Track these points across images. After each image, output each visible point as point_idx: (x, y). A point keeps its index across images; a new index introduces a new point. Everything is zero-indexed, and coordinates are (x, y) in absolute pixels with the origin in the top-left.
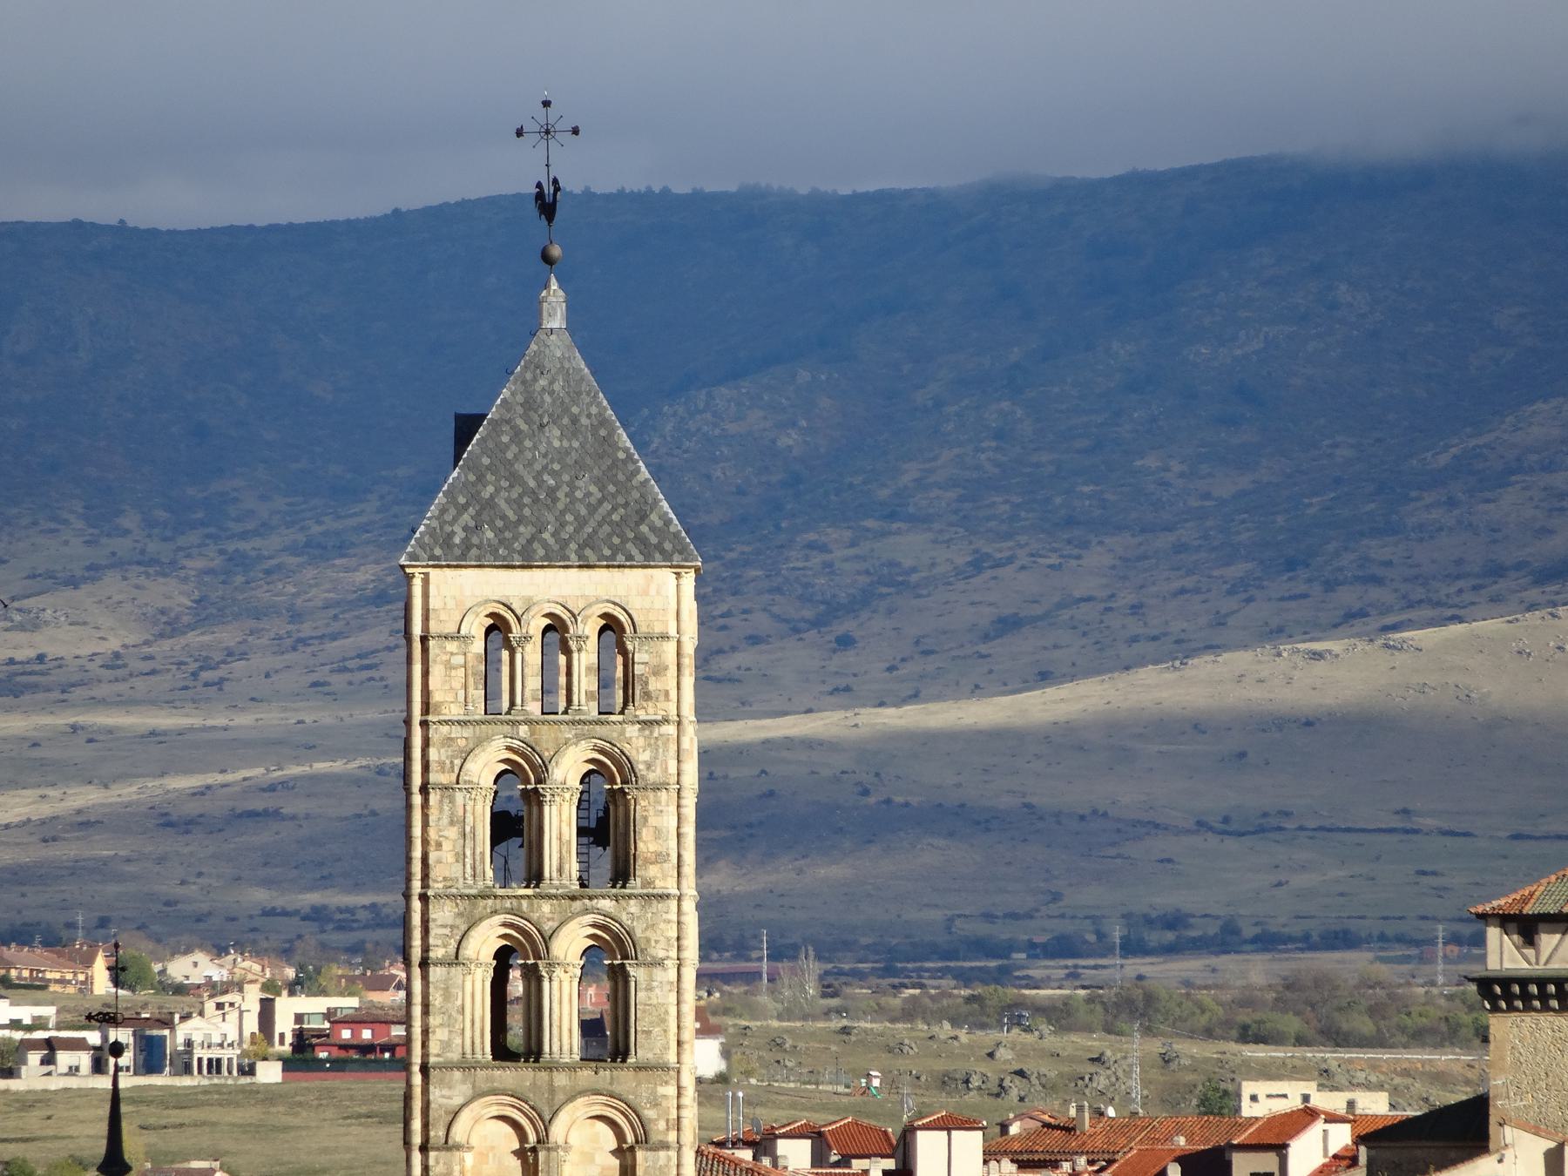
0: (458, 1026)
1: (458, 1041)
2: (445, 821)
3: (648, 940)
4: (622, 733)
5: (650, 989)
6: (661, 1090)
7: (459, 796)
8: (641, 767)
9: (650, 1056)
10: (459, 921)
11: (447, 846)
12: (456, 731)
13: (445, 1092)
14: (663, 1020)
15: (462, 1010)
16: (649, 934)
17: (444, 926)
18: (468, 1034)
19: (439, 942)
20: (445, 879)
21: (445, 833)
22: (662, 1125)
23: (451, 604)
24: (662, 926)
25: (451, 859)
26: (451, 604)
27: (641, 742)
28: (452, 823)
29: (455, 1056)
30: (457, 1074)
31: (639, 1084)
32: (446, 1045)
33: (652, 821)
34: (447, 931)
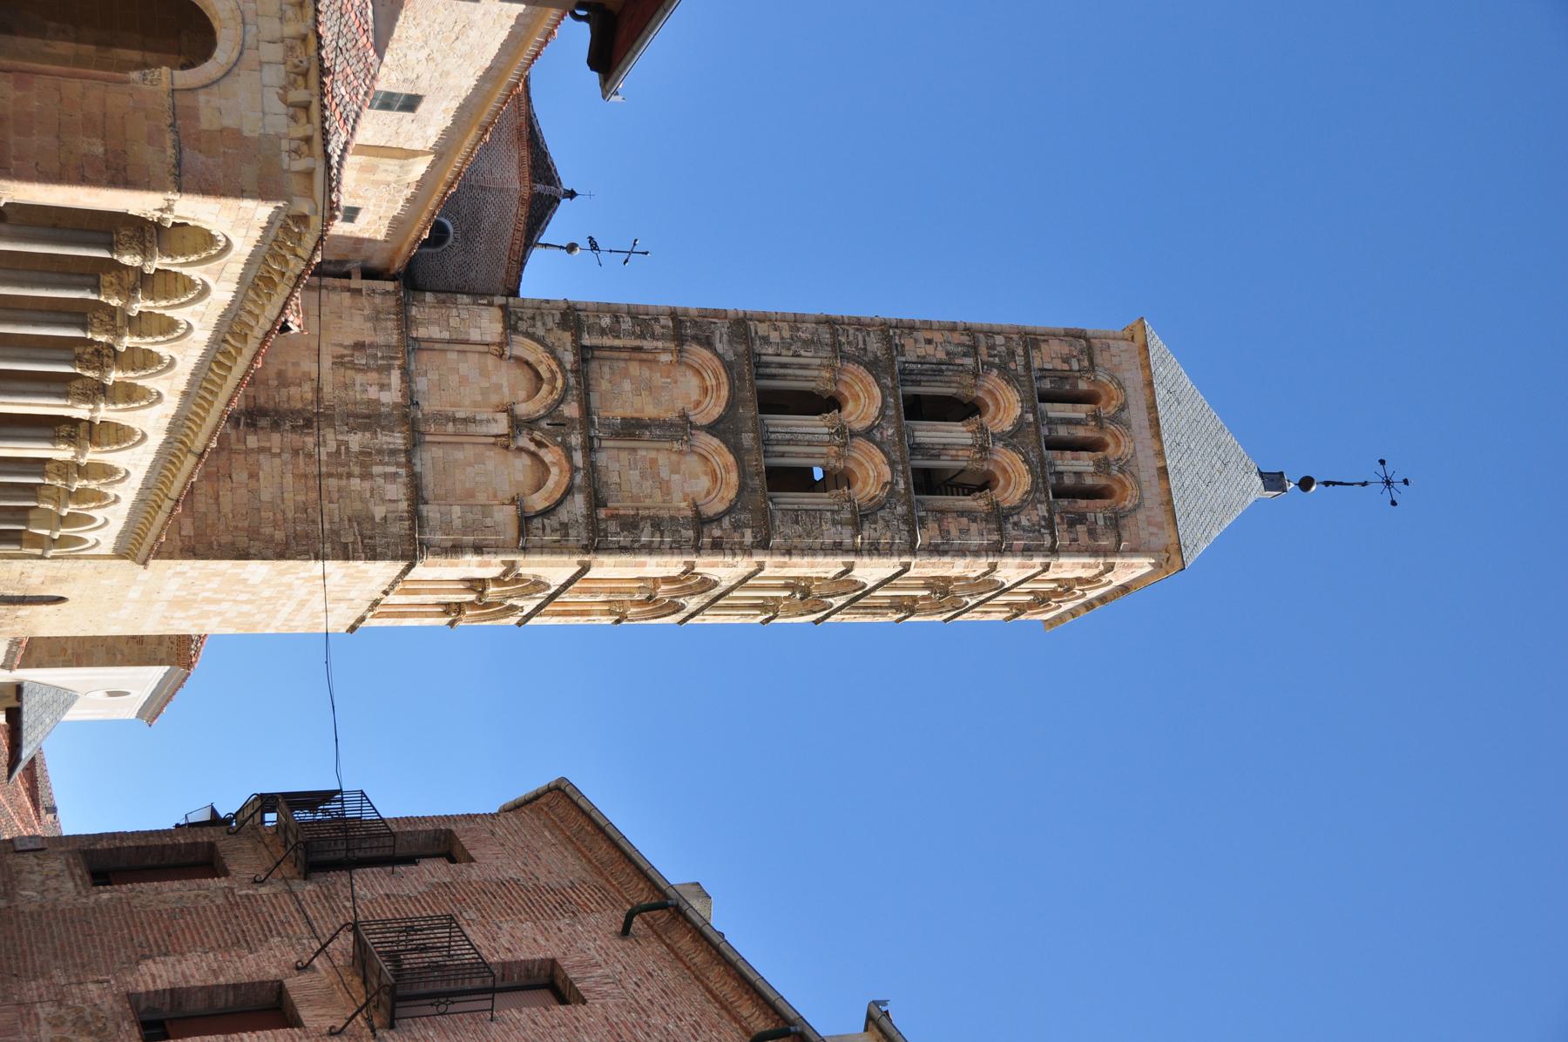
0: (784, 352)
1: (770, 351)
2: (951, 348)
3: (875, 522)
4: (1041, 502)
5: (835, 523)
6: (748, 533)
7: (969, 361)
8: (1016, 518)
10: (870, 355)
11: (930, 349)
12: (1020, 360)
13: (725, 337)
14: (808, 535)
15: (796, 355)
18: (777, 359)
22: (717, 533)
23: (1116, 360)
24: (889, 534)
25: (921, 352)
26: (1116, 360)
27: (1035, 519)
28: (948, 354)
29: (758, 347)
32: (766, 340)
33: (974, 527)
34: (861, 345)
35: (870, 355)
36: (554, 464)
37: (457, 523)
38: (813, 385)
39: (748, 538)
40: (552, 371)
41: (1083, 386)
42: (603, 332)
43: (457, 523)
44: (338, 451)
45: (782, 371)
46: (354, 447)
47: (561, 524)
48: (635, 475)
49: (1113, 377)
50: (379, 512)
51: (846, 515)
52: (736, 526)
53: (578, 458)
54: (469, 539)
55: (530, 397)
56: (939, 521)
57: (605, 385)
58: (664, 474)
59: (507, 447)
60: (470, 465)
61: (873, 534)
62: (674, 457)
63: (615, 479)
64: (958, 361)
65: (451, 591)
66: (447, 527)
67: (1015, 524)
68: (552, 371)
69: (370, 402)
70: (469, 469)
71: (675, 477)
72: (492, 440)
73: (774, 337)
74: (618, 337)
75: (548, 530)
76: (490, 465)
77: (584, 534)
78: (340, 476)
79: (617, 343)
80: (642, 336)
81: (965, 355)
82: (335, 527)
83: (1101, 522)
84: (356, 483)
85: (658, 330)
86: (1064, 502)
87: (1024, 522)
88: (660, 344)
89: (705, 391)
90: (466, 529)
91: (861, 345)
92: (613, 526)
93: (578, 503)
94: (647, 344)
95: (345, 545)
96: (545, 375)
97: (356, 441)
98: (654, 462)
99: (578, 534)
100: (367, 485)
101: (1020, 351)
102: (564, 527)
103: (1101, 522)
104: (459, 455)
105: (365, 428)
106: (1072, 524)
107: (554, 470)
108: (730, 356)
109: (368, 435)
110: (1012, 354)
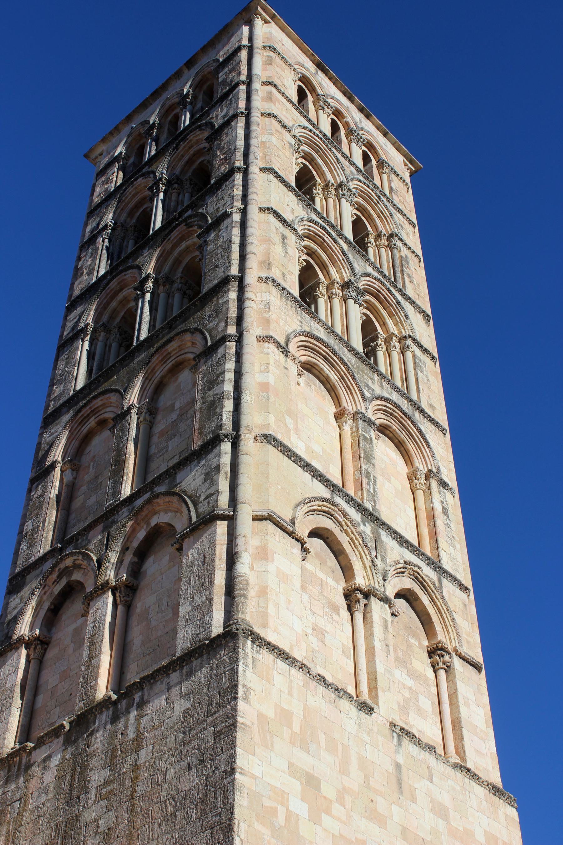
36: (148, 523)
38: (114, 345)
40: (60, 577)
44: (107, 797)
46: (106, 773)
50: (181, 706)
58: (174, 416)
65: (369, 635)
68: (60, 577)
69: (59, 778)
70: (153, 623)
71: (178, 405)
78: (135, 781)
82: (194, 761)
84: (144, 755)
95: (218, 735)
96: (64, 582)
97: (97, 776)
100: (148, 737)
105: (85, 768)
107: (154, 521)
109: (93, 763)
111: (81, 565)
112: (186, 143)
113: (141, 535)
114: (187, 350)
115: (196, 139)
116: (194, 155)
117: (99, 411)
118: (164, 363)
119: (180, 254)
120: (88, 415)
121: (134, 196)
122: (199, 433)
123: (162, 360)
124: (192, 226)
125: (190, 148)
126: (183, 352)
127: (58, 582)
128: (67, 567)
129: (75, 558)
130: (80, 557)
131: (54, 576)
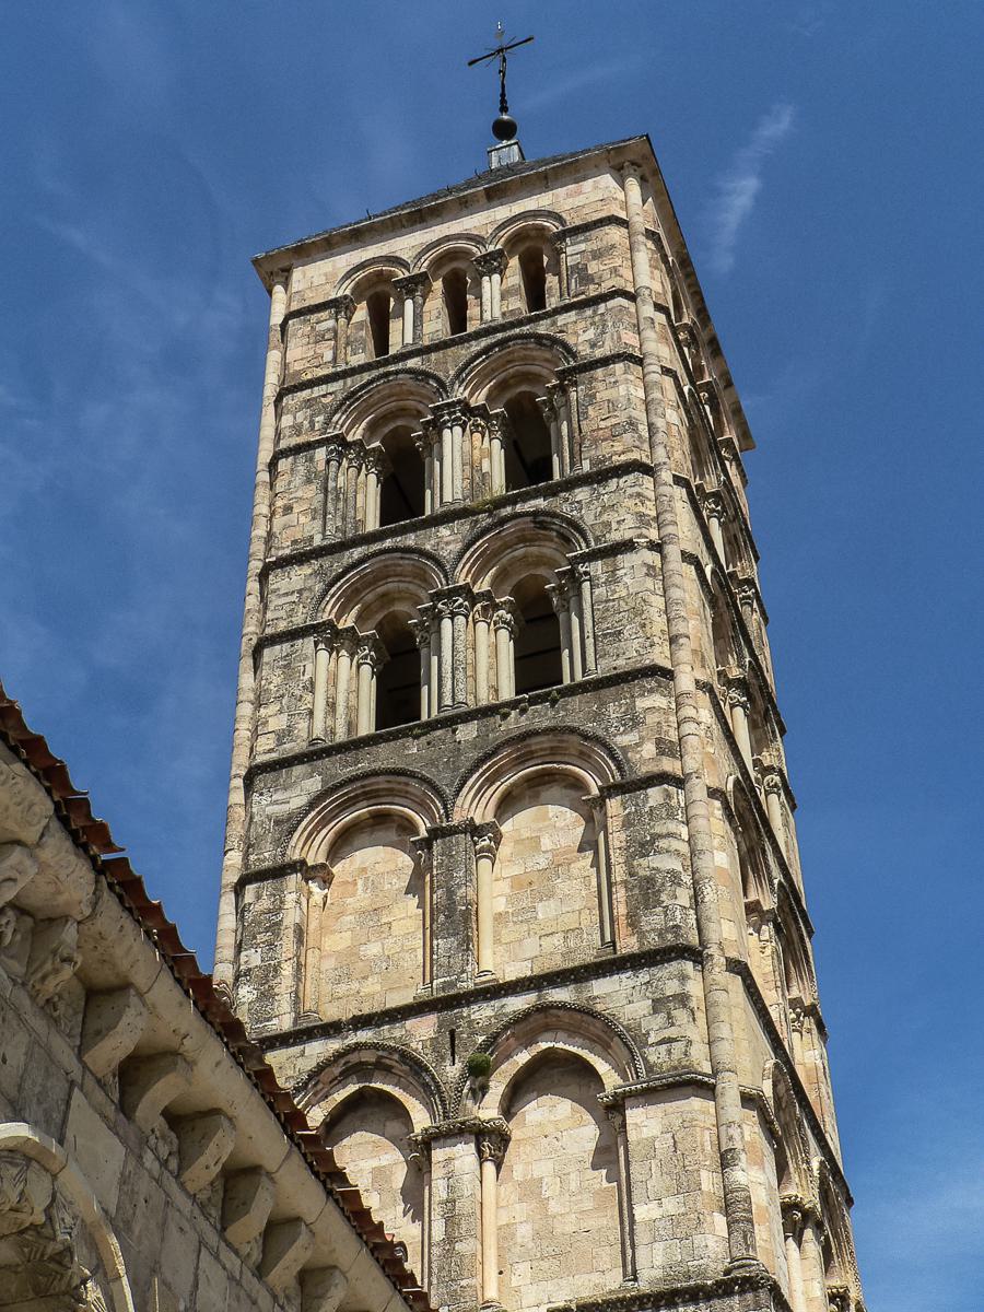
2: (298, 480)
5: (613, 579)
6: (641, 704)
8: (584, 350)
9: (621, 662)
12: (318, 391)
15: (311, 687)
16: (605, 517)
17: (286, 594)
19: (282, 613)
20: (295, 542)
21: (299, 494)
22: (649, 749)
28: (309, 481)
30: (298, 770)
31: (603, 704)
32: (281, 736)
34: (294, 598)
35: (310, 583)
37: (671, 1206)
39: (658, 701)
41: (361, 313)
42: (267, 996)
43: (671, 1206)
45: (341, 709)
47: (655, 1011)
48: (546, 910)
49: (348, 276)
51: (597, 568)
52: (633, 721)
53: (518, 1003)
54: (709, 1181)
55: (403, 1114)
56: (595, 441)
57: (372, 986)
58: (543, 862)
59: (503, 1140)
60: (544, 1202)
61: (630, 521)
62: (504, 850)
63: (557, 940)
64: (321, 466)
66: (683, 1228)
67: (593, 345)
70: (554, 1207)
72: (489, 1167)
73: (278, 723)
74: (277, 969)
75: (672, 1032)
76: (543, 1169)
77: (674, 967)
79: (287, 970)
80: (275, 928)
81: (311, 460)
83: (582, 247)
85: (265, 903)
86: (552, 302)
87: (591, 334)
88: (290, 898)
89: (380, 820)
90: (685, 1185)
91: (294, 598)
92: (653, 920)
93: (617, 995)
94: (291, 917)
98: (517, 883)
99: (668, 979)
101: (305, 394)
102: (658, 1005)
103: (582, 247)
104: (524, 1232)
106: (586, 279)
108: (314, 784)
110: (308, 403)
111: (393, 1067)
112: (504, 352)
113: (523, 1057)
114: (566, 759)
115: (525, 352)
116: (513, 377)
117: (379, 796)
118: (520, 763)
119: (512, 563)
120: (356, 796)
121: (383, 399)
122: (629, 925)
123: (517, 758)
124: (545, 529)
125: (509, 362)
126: (558, 758)
127: (340, 1082)
128: (361, 1063)
129: (380, 1053)
130: (396, 1057)
131: (336, 1070)
